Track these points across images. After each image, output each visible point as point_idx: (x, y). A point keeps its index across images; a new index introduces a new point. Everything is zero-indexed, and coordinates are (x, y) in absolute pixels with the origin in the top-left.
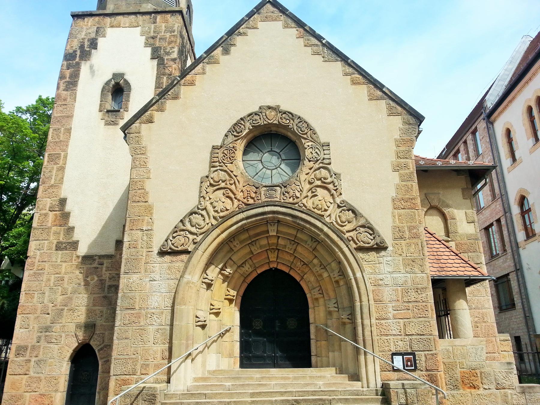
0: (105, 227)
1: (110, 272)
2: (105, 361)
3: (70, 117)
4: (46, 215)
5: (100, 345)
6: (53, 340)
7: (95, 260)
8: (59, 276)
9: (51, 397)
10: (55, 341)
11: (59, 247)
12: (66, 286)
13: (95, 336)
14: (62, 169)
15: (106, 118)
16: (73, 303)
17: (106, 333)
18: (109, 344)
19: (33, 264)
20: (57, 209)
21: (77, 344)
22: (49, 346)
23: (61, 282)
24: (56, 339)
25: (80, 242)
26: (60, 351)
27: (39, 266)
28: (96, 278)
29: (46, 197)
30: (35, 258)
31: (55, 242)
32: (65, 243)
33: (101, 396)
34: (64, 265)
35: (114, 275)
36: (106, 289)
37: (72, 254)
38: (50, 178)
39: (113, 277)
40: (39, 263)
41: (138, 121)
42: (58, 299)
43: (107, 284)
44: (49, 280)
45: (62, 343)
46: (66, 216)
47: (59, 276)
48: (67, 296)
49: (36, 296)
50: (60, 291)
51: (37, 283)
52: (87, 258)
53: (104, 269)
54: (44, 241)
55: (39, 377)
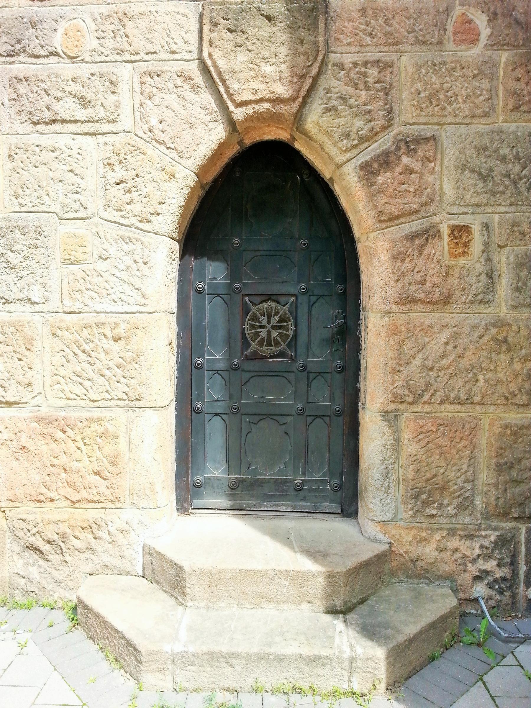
2: (412, 237)
5: (371, 137)
6: (67, 108)
9: (104, 435)
10: (82, 114)
13: (333, 83)
17: (406, 63)
18: (428, 131)
21: (219, 133)
22: (45, 141)
24: (84, 102)
26: (119, 173)
33: (406, 435)
45: (126, 121)
55: (18, 327)
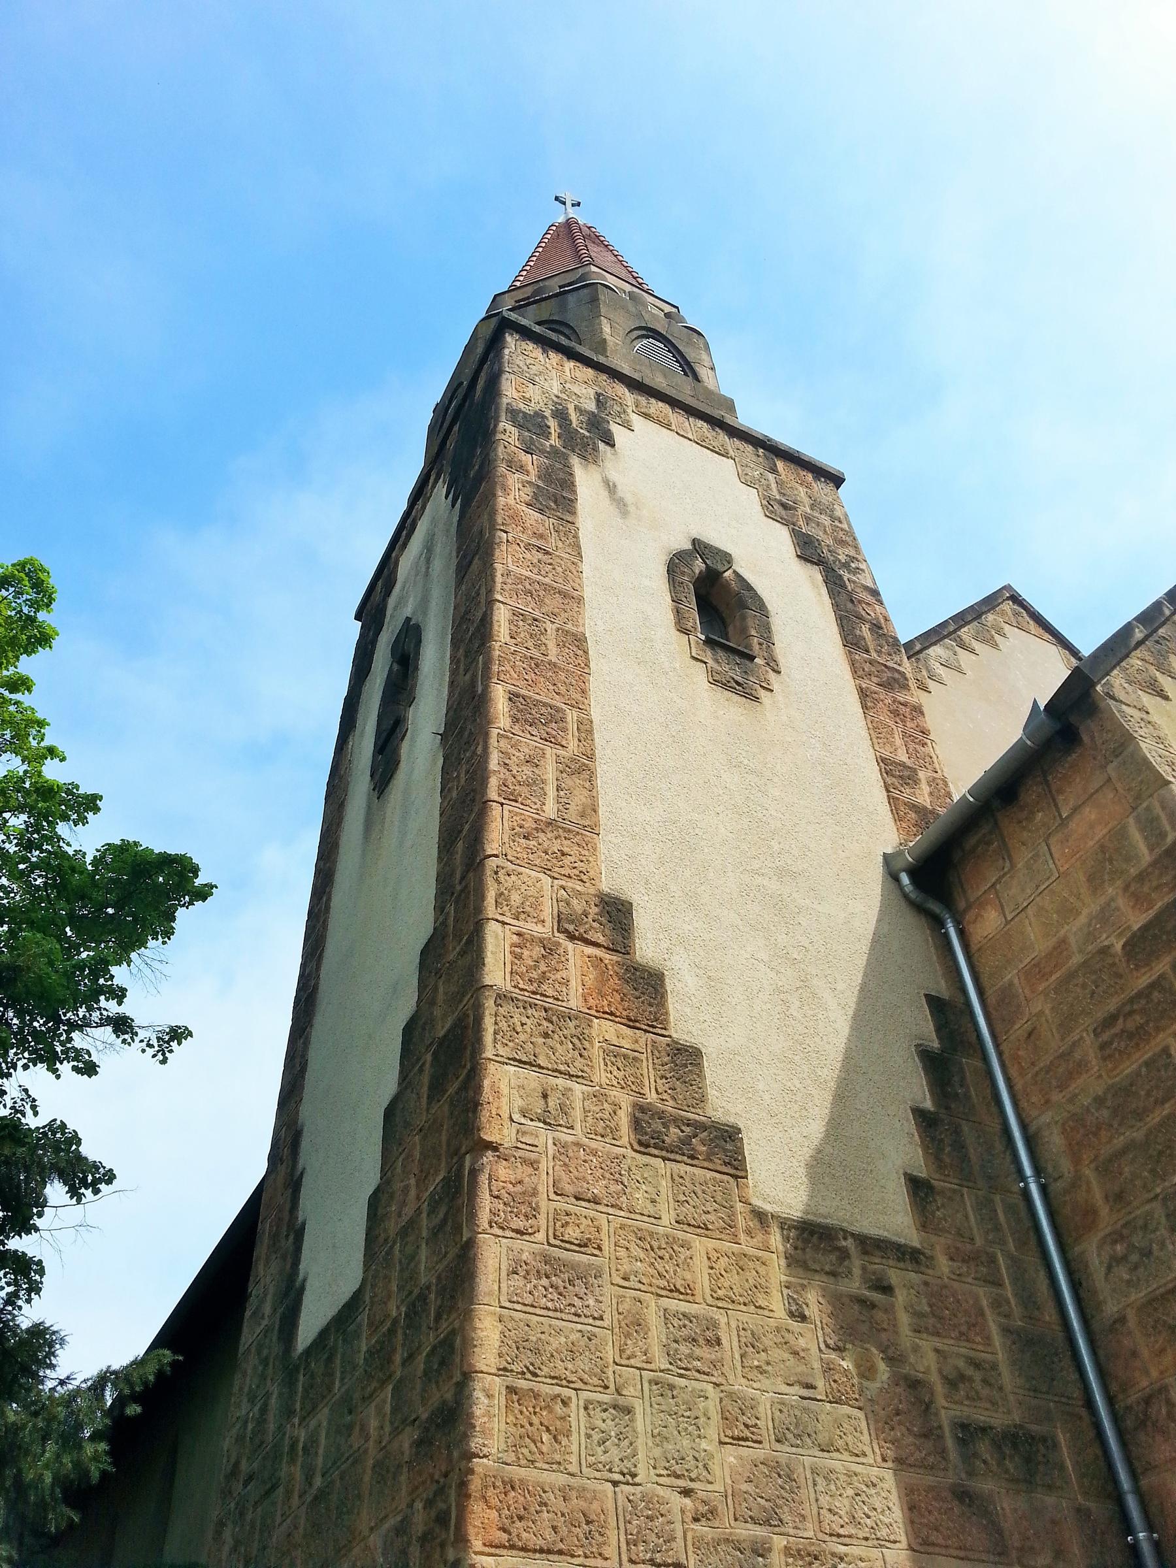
0: (842, 1096)
1: (937, 1343)
3: (572, 598)
4: (550, 949)
7: (844, 1255)
8: (684, 1307)
11: (650, 1131)
12: (739, 1385)
14: (581, 768)
15: (711, 662)
16: (809, 1509)
19: (523, 1201)
20: (601, 939)
23: (704, 1352)
25: (743, 1135)
27: (560, 1219)
28: (883, 1370)
29: (531, 865)
30: (533, 1164)
31: (625, 1101)
32: (678, 1121)
34: (701, 1245)
35: (961, 1364)
36: (950, 1443)
37: (726, 1192)
38: (536, 784)
39: (962, 1377)
40: (561, 1204)
41: (1115, 672)
42: (715, 1468)
43: (947, 1412)
44: (637, 1324)
46: (644, 990)
47: (684, 1307)
48: (760, 1453)
49: (577, 1418)
50: (712, 1406)
51: (572, 1331)
52: (815, 1242)
53: (904, 1320)
54: (561, 1082)
